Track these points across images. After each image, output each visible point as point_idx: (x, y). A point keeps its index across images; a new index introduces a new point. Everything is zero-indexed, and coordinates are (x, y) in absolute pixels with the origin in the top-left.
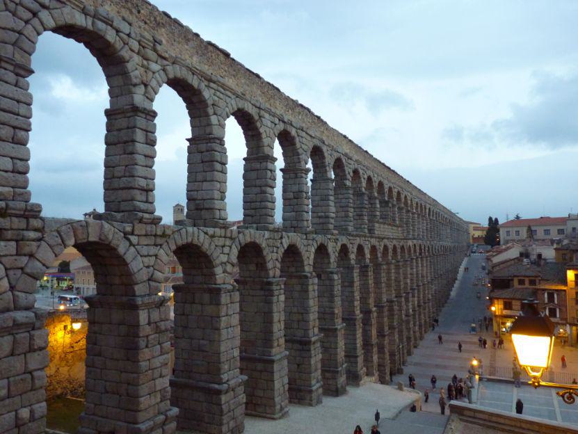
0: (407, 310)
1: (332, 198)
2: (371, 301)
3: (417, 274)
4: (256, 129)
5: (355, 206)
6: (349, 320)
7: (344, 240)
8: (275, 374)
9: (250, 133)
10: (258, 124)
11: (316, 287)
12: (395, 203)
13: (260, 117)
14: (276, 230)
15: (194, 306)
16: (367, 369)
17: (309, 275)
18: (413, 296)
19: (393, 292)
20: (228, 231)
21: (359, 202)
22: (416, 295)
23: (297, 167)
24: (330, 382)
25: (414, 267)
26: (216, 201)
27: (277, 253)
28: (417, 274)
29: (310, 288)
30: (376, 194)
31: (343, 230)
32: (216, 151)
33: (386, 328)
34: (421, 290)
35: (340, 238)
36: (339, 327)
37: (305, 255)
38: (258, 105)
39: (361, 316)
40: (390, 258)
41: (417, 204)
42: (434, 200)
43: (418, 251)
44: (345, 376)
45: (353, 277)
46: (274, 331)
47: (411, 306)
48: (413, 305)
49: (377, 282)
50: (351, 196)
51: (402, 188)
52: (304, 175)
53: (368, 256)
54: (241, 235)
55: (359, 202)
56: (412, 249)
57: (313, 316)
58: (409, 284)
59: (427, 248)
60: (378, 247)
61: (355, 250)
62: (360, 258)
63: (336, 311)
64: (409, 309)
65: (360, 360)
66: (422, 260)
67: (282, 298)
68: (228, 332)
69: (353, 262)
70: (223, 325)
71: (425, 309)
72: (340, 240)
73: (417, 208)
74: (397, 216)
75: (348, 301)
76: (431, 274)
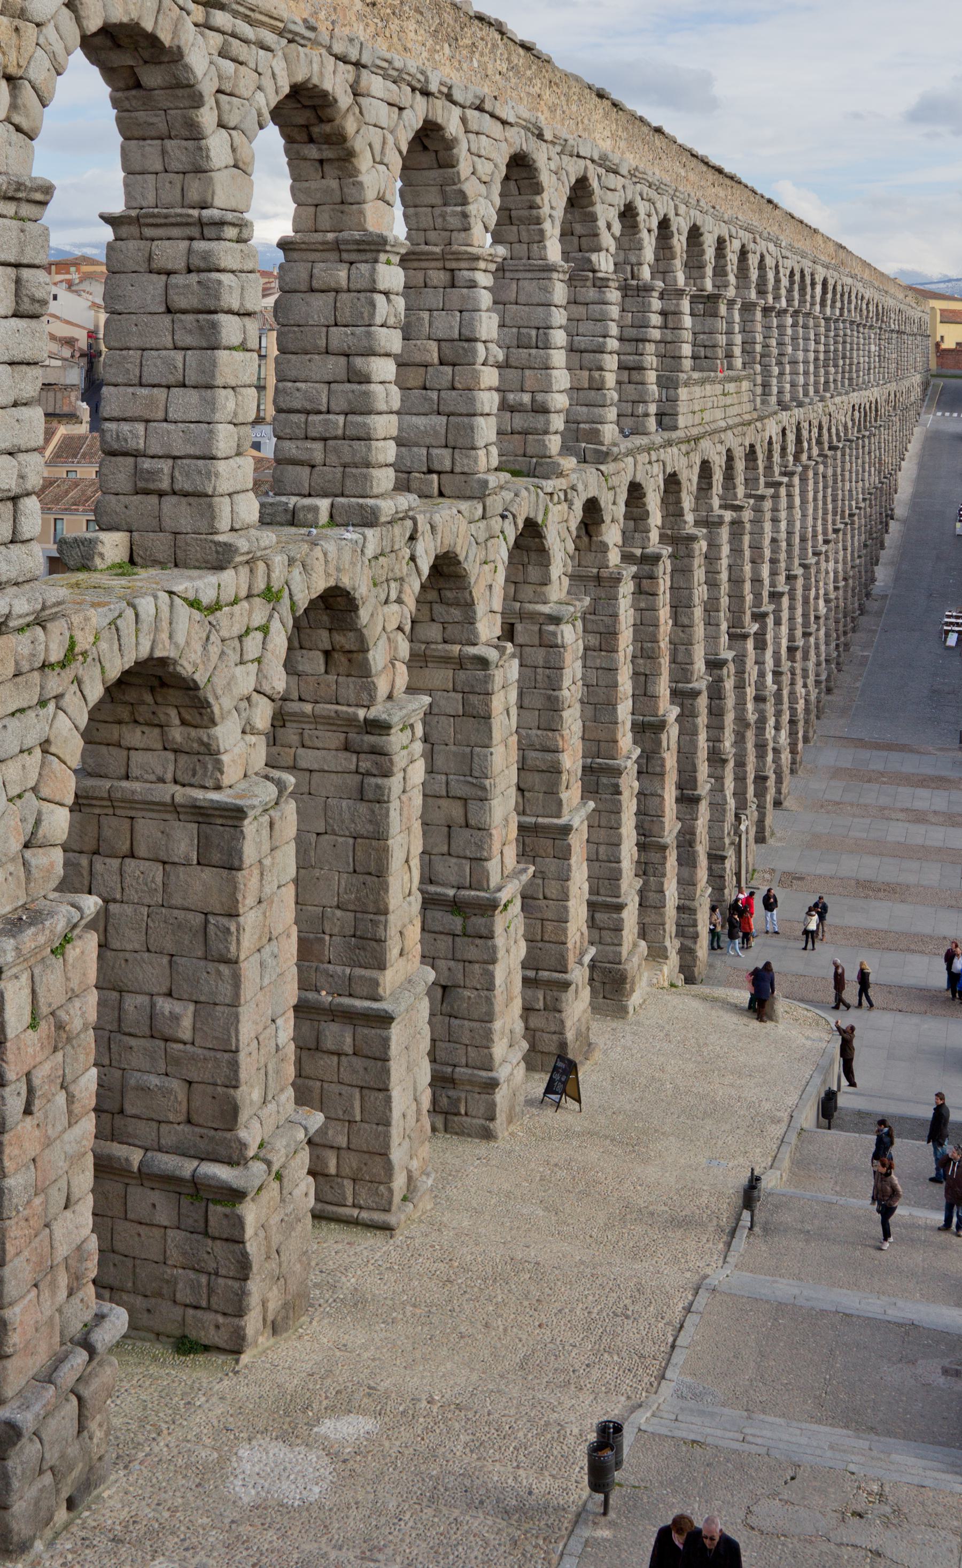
2: (663, 688)
6: (599, 778)
7: (589, 482)
13: (355, 95)
17: (492, 655)
23: (455, 248)
26: (221, 466)
27: (399, 601)
38: (354, 55)
41: (792, 274)
43: (791, 448)
45: (615, 616)
49: (680, 606)
53: (656, 518)
56: (777, 447)
58: (767, 582)
61: (622, 508)
66: (804, 480)
67: (418, 772)
69: (614, 557)
71: (806, 658)
72: (580, 487)
74: (738, 339)
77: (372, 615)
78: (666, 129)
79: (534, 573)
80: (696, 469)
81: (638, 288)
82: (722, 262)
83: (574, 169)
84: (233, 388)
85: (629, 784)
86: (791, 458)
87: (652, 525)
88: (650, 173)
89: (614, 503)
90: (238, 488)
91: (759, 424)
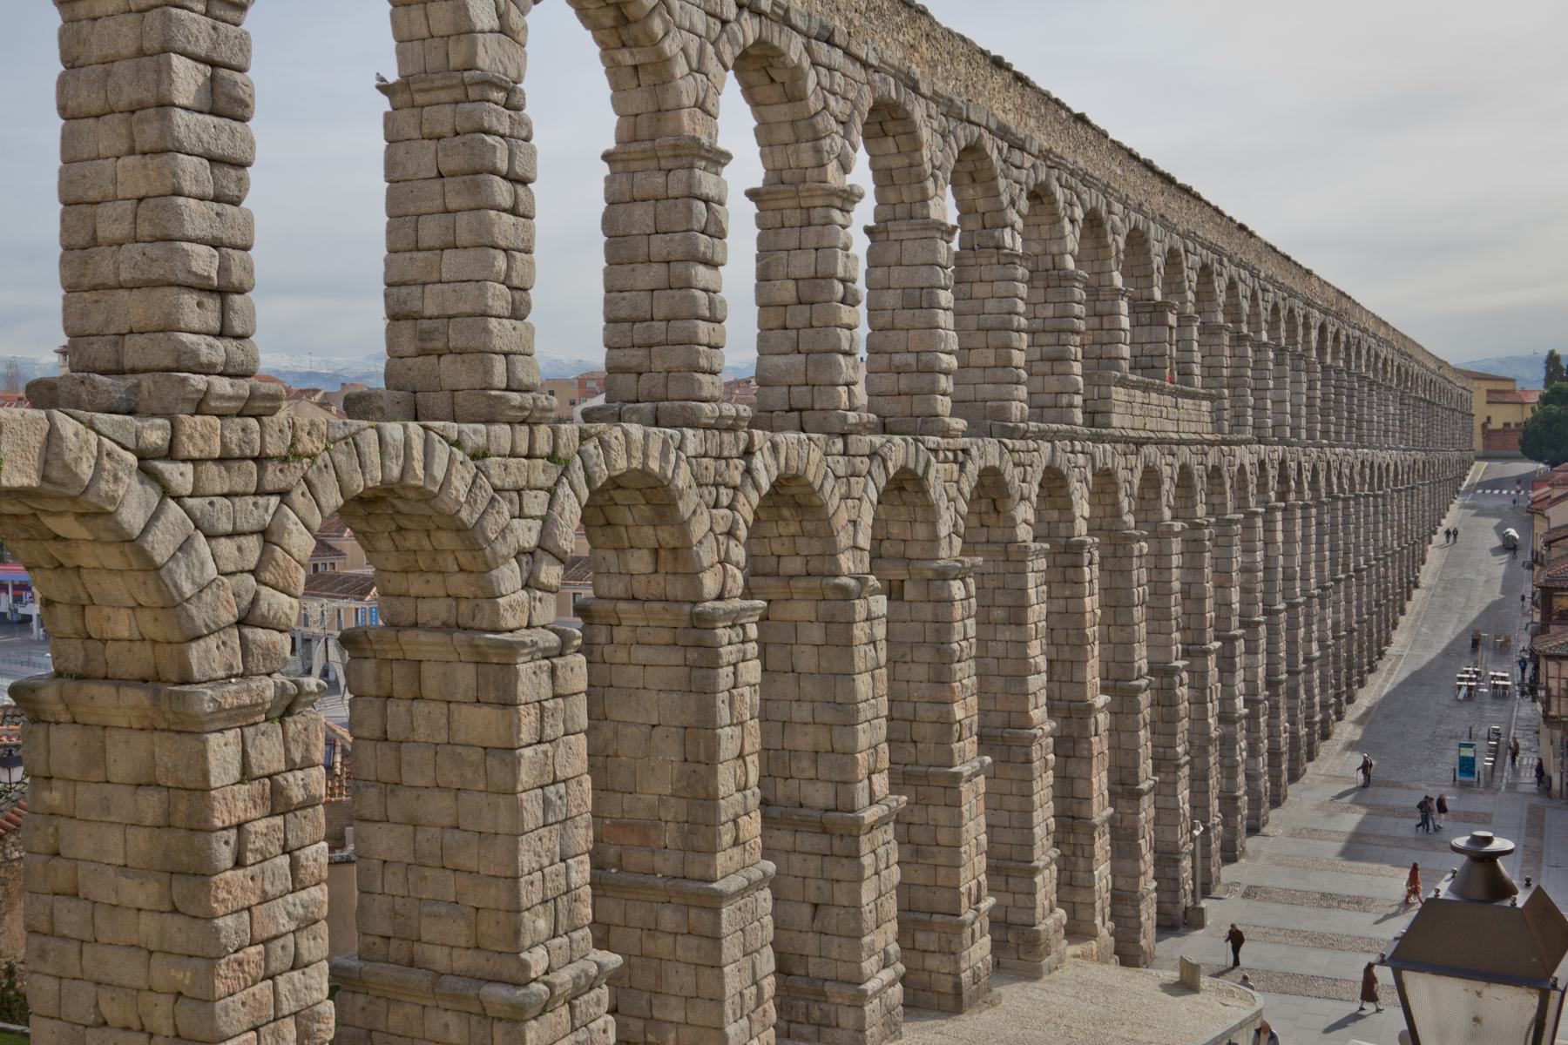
0: (1227, 699)
1: (946, 298)
2: (1093, 672)
3: (1269, 569)
4: (655, 43)
5: (1038, 324)
7: (988, 452)
8: (725, 943)
9: (625, 57)
10: (657, 26)
11: (880, 631)
12: (1190, 309)
14: (727, 426)
15: (420, 708)
16: (1072, 915)
18: (1251, 651)
19: (1176, 636)
20: (543, 432)
21: (1049, 311)
22: (1263, 643)
24: (932, 962)
25: (1260, 545)
26: (493, 322)
27: (731, 507)
28: (1269, 569)
29: (860, 632)
30: (1118, 280)
31: (988, 420)
32: (487, 132)
33: (1146, 767)
34: (1283, 626)
35: (974, 445)
36: (966, 770)
37: (842, 519)
39: (1050, 726)
40: (1167, 514)
42: (1343, 294)
43: (1272, 483)
44: (986, 941)
45: (1023, 590)
46: (722, 791)
47: (1240, 686)
48: (1250, 682)
49: (1116, 603)
50: (1022, 289)
51: (1211, 248)
52: (837, 215)
53: (1082, 508)
54: (590, 446)
55: (1049, 311)
56: (1252, 480)
57: (870, 734)
58: (1236, 606)
59: (1307, 476)
60: (1122, 474)
62: (1055, 515)
63: (959, 714)
64: (1233, 697)
65: (1046, 883)
67: (752, 671)
68: (546, 802)
69: (1024, 533)
70: (526, 776)
72: (974, 451)
73: (1273, 327)
74: (1197, 357)
75: (1001, 677)
76: (1320, 569)
77: (694, 512)
78: (1089, 116)
79: (921, 531)
80: (1138, 473)
81: (1060, 278)
82: (1178, 278)
83: (963, 134)
84: (505, 250)
85: (1043, 755)
86: (1272, 494)
87: (1078, 514)
88: (1071, 160)
89: (1024, 481)
90: (515, 349)
91: (1225, 448)
